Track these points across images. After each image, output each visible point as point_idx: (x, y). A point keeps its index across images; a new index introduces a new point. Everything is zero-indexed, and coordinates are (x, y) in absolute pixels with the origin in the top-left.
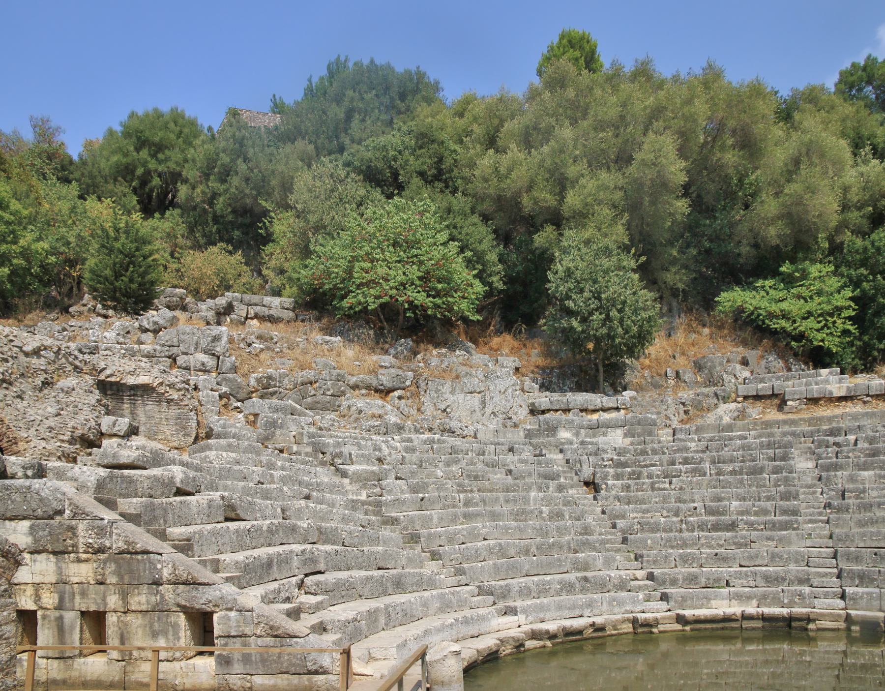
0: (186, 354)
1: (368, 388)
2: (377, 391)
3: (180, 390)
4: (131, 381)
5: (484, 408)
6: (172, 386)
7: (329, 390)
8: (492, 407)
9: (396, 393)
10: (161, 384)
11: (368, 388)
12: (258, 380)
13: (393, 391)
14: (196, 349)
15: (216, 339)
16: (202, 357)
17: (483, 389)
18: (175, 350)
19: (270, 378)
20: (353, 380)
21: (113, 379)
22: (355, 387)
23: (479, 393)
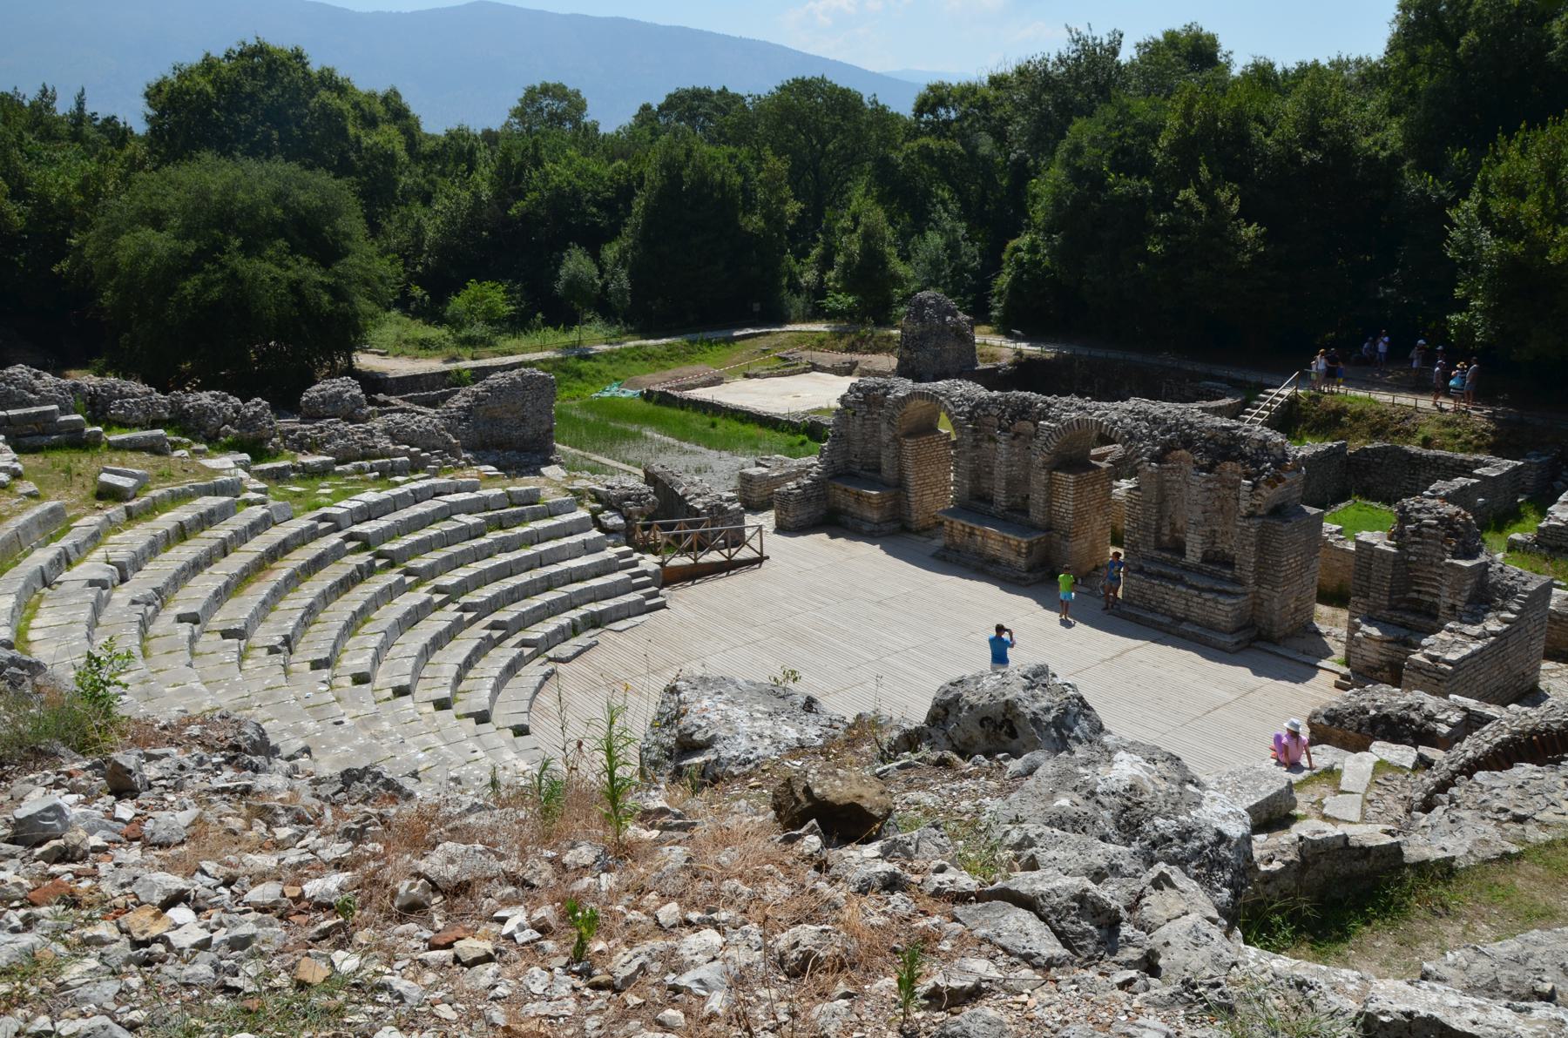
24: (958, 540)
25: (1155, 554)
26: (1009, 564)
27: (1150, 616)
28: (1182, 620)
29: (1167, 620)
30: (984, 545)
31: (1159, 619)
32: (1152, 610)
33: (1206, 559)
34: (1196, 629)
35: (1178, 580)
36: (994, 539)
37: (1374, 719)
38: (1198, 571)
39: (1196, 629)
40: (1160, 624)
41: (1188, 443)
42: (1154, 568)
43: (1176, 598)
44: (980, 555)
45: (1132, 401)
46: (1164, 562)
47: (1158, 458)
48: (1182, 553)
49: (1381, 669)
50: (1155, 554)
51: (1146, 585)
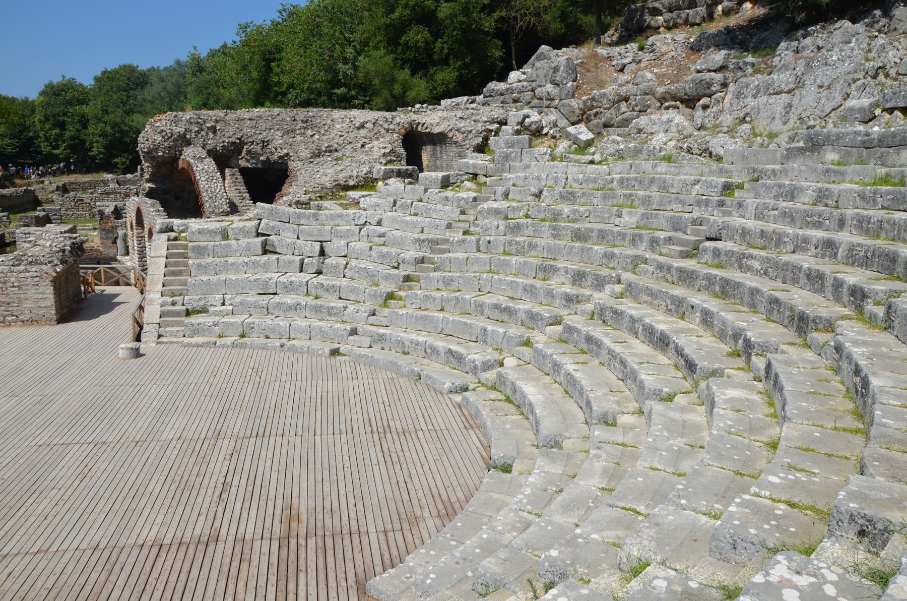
0: (540, 86)
1: (674, 98)
2: (682, 101)
3: (464, 133)
4: (436, 130)
5: (788, 113)
6: (458, 130)
7: (637, 106)
8: (799, 111)
9: (701, 102)
10: (451, 130)
11: (674, 98)
12: (585, 102)
13: (699, 100)
14: (546, 80)
15: (556, 69)
16: (549, 87)
17: (791, 86)
18: (534, 84)
19: (593, 99)
20: (660, 90)
21: (427, 130)
22: (662, 99)
23: (789, 92)
37: (71, 252)
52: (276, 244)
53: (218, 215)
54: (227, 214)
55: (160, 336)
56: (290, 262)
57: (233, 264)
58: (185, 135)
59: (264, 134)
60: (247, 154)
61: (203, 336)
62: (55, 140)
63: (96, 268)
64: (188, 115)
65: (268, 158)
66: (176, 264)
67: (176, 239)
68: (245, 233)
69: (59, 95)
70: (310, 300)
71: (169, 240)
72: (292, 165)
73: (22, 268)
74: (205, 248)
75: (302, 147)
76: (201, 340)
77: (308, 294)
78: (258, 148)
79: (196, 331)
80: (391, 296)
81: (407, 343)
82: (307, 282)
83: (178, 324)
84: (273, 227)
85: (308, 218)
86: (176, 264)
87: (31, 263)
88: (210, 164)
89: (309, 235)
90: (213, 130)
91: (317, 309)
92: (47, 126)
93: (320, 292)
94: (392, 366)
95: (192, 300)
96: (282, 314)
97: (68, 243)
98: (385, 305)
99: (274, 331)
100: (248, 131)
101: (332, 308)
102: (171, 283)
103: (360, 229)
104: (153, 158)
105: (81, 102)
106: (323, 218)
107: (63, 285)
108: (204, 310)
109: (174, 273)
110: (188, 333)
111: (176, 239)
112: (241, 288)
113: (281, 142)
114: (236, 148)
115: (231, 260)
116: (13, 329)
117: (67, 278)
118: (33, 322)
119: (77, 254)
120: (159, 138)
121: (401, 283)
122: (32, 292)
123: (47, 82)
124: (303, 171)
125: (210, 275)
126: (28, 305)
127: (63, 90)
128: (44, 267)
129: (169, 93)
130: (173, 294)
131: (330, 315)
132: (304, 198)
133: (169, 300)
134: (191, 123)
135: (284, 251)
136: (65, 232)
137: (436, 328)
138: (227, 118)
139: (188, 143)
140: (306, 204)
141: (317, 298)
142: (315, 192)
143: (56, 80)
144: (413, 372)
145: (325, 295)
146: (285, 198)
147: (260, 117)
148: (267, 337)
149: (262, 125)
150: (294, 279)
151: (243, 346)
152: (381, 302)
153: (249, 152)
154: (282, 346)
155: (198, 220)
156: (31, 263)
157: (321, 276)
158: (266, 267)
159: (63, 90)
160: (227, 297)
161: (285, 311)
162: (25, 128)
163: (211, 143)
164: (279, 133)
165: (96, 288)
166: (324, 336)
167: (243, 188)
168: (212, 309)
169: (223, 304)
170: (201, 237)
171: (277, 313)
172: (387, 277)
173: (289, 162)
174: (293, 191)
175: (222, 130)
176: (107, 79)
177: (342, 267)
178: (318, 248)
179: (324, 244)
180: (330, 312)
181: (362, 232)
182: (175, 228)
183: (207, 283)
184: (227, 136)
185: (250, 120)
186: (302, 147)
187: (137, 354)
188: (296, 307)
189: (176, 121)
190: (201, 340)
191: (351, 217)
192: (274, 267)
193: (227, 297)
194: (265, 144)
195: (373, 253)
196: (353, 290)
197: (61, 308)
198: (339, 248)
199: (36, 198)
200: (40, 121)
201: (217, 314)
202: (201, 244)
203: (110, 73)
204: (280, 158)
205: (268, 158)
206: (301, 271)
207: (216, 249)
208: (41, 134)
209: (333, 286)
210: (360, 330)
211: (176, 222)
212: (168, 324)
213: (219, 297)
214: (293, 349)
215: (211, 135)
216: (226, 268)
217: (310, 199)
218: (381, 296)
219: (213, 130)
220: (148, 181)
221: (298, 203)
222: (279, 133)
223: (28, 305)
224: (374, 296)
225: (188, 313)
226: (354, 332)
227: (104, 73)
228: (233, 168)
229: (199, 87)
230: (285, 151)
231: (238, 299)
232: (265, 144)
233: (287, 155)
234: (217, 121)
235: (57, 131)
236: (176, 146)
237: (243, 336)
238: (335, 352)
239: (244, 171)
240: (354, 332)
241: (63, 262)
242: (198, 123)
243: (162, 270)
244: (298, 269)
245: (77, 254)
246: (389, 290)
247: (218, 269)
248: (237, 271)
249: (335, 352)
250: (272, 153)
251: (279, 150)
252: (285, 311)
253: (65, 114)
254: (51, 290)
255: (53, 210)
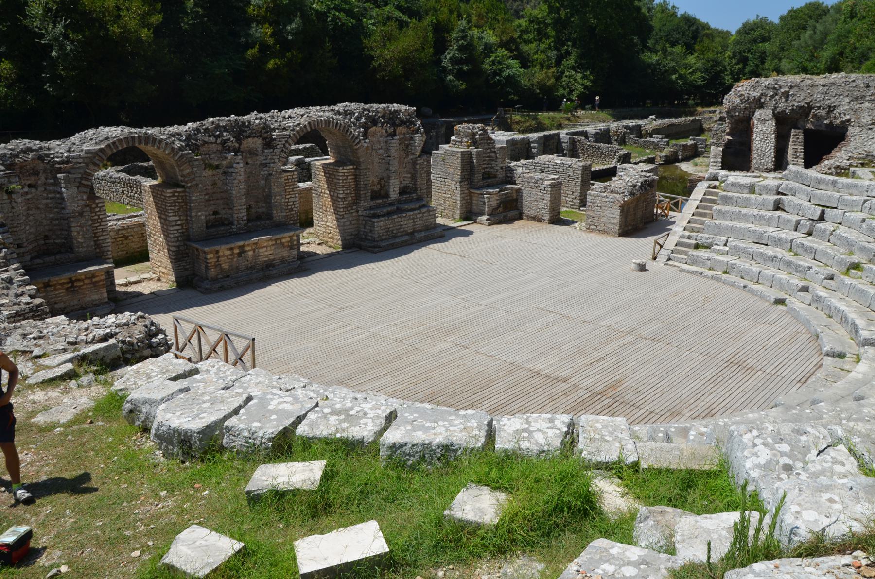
24: (225, 266)
25: (372, 203)
26: (283, 261)
27: (397, 240)
28: (412, 233)
29: (407, 237)
30: (256, 257)
31: (404, 239)
32: (394, 237)
33: (400, 194)
34: (423, 234)
35: (399, 211)
36: (264, 247)
37: (640, 187)
38: (399, 201)
39: (423, 234)
40: (406, 241)
41: (373, 121)
42: (385, 210)
43: (406, 222)
44: (252, 268)
45: (296, 109)
46: (378, 207)
47: (365, 135)
48: (387, 196)
49: (499, 207)
50: (372, 203)
51: (389, 222)
52: (786, 204)
53: (762, 171)
54: (769, 171)
55: (669, 259)
56: (789, 221)
57: (745, 215)
58: (760, 98)
59: (833, 99)
60: (812, 118)
61: (699, 266)
62: (738, 74)
63: (672, 199)
64: (766, 82)
65: (831, 122)
66: (705, 208)
67: (714, 187)
68: (767, 190)
69: (748, 34)
70: (788, 256)
71: (709, 187)
72: (851, 130)
73: (605, 194)
74: (731, 198)
75: (866, 114)
76: (694, 268)
77: (791, 250)
78: (823, 113)
79: (694, 261)
80: (856, 266)
81: (833, 308)
82: (792, 241)
83: (685, 253)
84: (791, 189)
85: (827, 184)
86: (705, 208)
87: (612, 192)
88: (770, 127)
89: (820, 200)
90: (786, 95)
91: (789, 264)
92: (734, 61)
93: (799, 251)
94: (806, 323)
95: (703, 237)
96: (762, 262)
97: (641, 180)
98: (847, 273)
99: (748, 273)
100: (818, 97)
101: (799, 266)
102: (695, 222)
103: (865, 201)
104: (732, 116)
105: (764, 40)
106: (839, 186)
107: (632, 210)
108: (708, 247)
109: (700, 215)
110: (689, 261)
111: (714, 187)
112: (741, 234)
113: (846, 107)
114: (805, 111)
115: (744, 211)
116: (592, 234)
117: (637, 205)
118: (604, 232)
119: (645, 189)
120: (738, 101)
121: (871, 257)
122: (607, 212)
123: (744, 21)
124: (857, 137)
125: (726, 220)
126: (604, 220)
127: (753, 29)
128: (618, 196)
129: (815, 41)
130: (692, 230)
131: (797, 271)
132: (846, 163)
133: (687, 233)
134: (768, 88)
135: (791, 210)
136: (645, 171)
137: (866, 301)
138: (802, 84)
139: (761, 106)
140: (846, 169)
141: (796, 255)
142: (858, 159)
143: (752, 18)
144: (816, 331)
145: (804, 253)
146: (826, 162)
147: (834, 84)
148: (742, 278)
149: (834, 91)
150: (783, 236)
151: (718, 280)
152: (845, 269)
153: (815, 115)
154: (745, 287)
155: (744, 174)
156: (612, 192)
157: (810, 238)
158: (768, 222)
159: (753, 29)
160: (730, 240)
161: (765, 260)
162: (716, 63)
163: (782, 106)
164: (847, 99)
165: (671, 213)
166: (782, 286)
167: (800, 148)
168: (715, 247)
169: (725, 245)
170: (733, 189)
171: (759, 260)
172: (863, 249)
173: (850, 128)
174: (840, 156)
175: (794, 95)
176: (794, 14)
177: (828, 232)
178: (819, 213)
179: (827, 210)
180: (798, 269)
181: (866, 205)
182: (720, 178)
183: (719, 227)
184: (799, 99)
185: (824, 86)
186: (866, 114)
187: (642, 268)
188: (773, 259)
189: (754, 88)
190: (694, 268)
191: (865, 189)
192: (775, 223)
193: (730, 240)
194: (831, 109)
195: (864, 225)
196: (825, 254)
197: (626, 226)
198: (836, 215)
199: (701, 125)
200: (729, 57)
201: (718, 252)
202: (729, 194)
203: (795, 11)
204: (842, 122)
205: (831, 122)
206: (796, 230)
207: (739, 200)
208: (728, 68)
209: (811, 248)
210: (810, 289)
211: (723, 173)
212: (679, 252)
213: (724, 238)
214: (751, 291)
215: (783, 100)
216: (739, 217)
217: (851, 165)
218: (846, 264)
219: (786, 95)
220: (728, 134)
221: (838, 167)
222: (847, 99)
223: (604, 220)
224: (841, 263)
225: (697, 247)
226: (805, 289)
227: (790, 12)
228: (799, 129)
229: (838, 36)
230: (848, 117)
231: (733, 244)
232: (831, 109)
233: (849, 120)
234: (791, 87)
235: (740, 66)
236: (750, 107)
237: (725, 273)
238: (780, 302)
239: (807, 133)
240: (805, 289)
241: (631, 194)
242: (774, 88)
243: (693, 210)
244: (793, 228)
245: (645, 189)
246: (856, 261)
247: (733, 216)
248: (747, 221)
249: (780, 302)
250: (835, 118)
251: (842, 115)
252: (765, 260)
253: (749, 51)
254: (618, 212)
255: (700, 140)
